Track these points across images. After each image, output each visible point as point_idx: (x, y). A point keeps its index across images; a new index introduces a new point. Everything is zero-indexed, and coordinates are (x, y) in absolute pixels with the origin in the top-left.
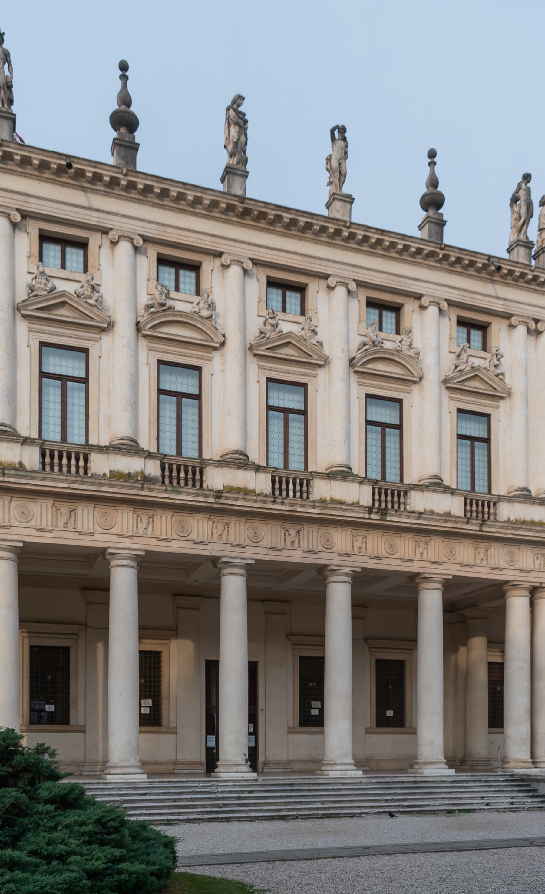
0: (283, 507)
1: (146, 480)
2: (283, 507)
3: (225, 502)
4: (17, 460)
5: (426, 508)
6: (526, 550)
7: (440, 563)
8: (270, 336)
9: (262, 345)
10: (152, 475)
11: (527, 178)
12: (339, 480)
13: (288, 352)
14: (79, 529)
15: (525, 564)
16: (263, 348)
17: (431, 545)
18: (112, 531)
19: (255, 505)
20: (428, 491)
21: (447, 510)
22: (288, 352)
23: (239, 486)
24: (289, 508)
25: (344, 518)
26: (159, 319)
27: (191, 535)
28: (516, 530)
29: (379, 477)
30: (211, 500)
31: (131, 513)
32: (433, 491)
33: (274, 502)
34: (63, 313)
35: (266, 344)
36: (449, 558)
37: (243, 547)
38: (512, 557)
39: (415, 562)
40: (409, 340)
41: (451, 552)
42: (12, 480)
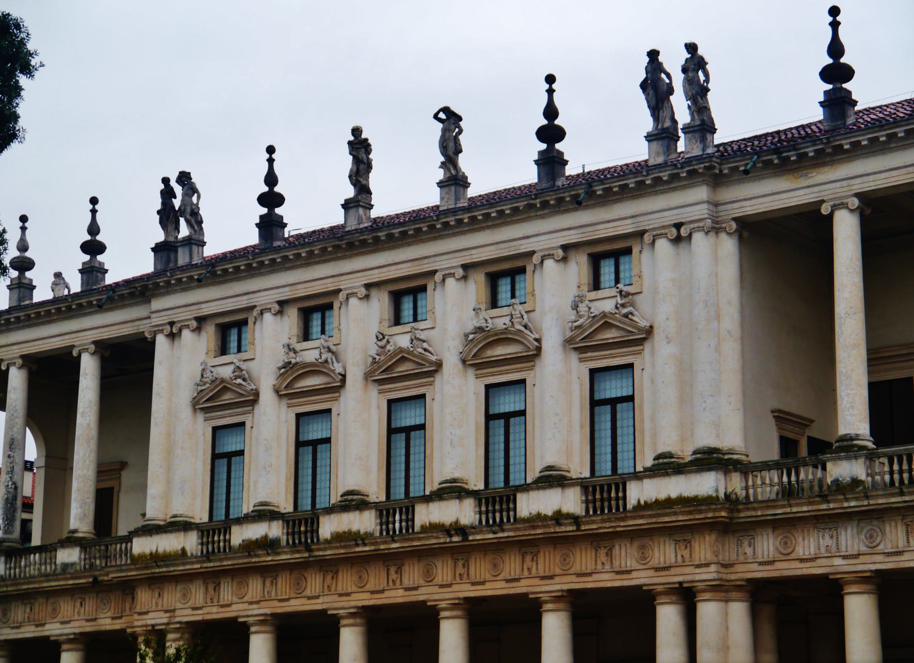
0: (367, 548)
1: (267, 544)
2: (367, 548)
3: (321, 553)
4: (179, 547)
5: (531, 511)
6: (662, 540)
7: (551, 577)
8: (380, 359)
9: (375, 370)
10: (275, 537)
11: (653, 55)
12: (436, 500)
13: (404, 368)
14: (221, 603)
15: (662, 559)
16: (377, 373)
17: (406, 569)
18: (246, 599)
19: (342, 551)
20: (533, 489)
21: (556, 508)
22: (404, 368)
23: (343, 530)
24: (373, 548)
25: (428, 547)
26: (292, 375)
27: (306, 591)
29: (481, 486)
30: (306, 555)
31: (259, 578)
32: (538, 488)
33: (357, 545)
34: (227, 397)
35: (380, 367)
36: (564, 568)
37: (348, 594)
38: (643, 553)
39: (487, 584)
40: (518, 312)
41: (565, 560)
42: (164, 570)
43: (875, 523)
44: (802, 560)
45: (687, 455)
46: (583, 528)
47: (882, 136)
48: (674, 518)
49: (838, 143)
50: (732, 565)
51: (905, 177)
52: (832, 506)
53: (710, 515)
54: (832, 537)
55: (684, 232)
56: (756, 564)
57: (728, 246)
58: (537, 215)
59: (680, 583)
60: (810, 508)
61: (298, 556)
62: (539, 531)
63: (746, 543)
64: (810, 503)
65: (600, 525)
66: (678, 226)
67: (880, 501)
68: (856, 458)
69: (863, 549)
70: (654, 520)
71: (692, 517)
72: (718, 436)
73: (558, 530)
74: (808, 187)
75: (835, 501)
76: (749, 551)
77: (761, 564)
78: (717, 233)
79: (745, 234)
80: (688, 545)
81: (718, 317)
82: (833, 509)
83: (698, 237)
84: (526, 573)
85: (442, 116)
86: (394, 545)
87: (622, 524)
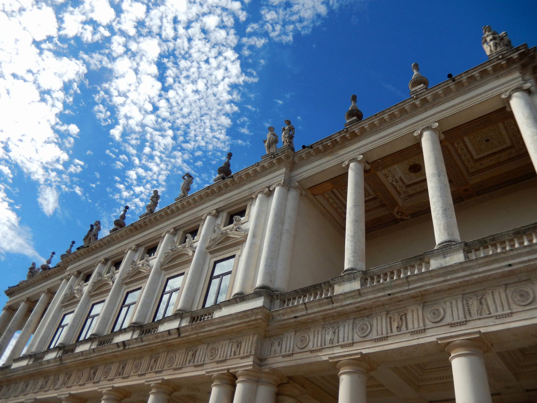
28: (204, 328)
43: (366, 319)
44: (312, 351)
45: (249, 291)
46: (182, 335)
47: (376, 121)
48: (231, 323)
49: (353, 130)
50: (265, 360)
51: (389, 139)
52: (335, 305)
53: (253, 318)
54: (334, 333)
55: (271, 189)
56: (281, 357)
57: (293, 195)
58: (209, 199)
59: (228, 370)
60: (319, 309)
61: (56, 364)
62: (159, 340)
63: (276, 344)
64: (320, 305)
65: (190, 333)
66: (269, 187)
67: (370, 297)
68: (354, 279)
69: (357, 338)
70: (220, 326)
71: (242, 321)
72: (271, 281)
73: (169, 338)
74: (337, 158)
75: (337, 301)
76: (278, 349)
77: (284, 356)
78: (288, 190)
79: (304, 192)
80: (240, 345)
81: (283, 224)
82: (336, 308)
83: (277, 189)
84: (150, 369)
85: (186, 177)
86: (95, 355)
87: (203, 330)
